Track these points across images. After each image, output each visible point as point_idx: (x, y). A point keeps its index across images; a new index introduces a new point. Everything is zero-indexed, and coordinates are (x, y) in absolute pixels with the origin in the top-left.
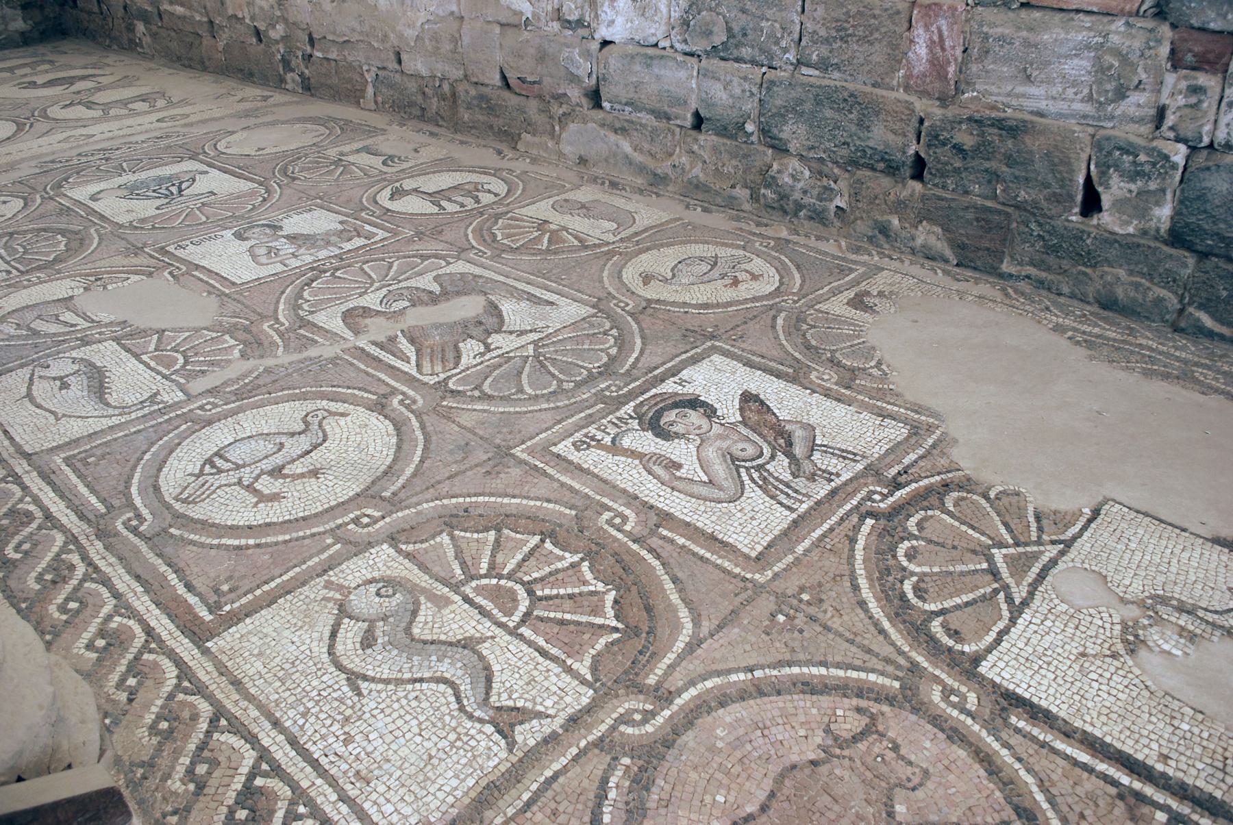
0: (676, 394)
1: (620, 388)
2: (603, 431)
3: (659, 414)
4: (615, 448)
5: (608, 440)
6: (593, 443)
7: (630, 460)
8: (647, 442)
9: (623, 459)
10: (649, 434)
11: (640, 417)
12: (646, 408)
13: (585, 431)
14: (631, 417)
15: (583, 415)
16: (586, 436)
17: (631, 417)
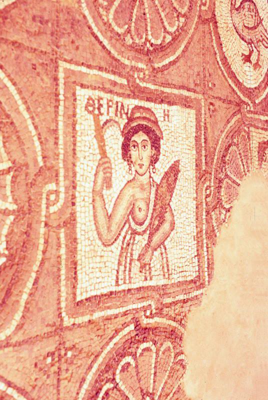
0: (156, 122)
1: (143, 80)
2: (109, 106)
3: (135, 131)
4: (100, 129)
5: (103, 119)
6: (96, 112)
7: (97, 151)
8: (114, 139)
9: (96, 146)
10: (122, 139)
11: (130, 120)
12: (137, 115)
13: (102, 94)
14: (127, 114)
15: (112, 77)
16: (100, 99)
17: (127, 114)
